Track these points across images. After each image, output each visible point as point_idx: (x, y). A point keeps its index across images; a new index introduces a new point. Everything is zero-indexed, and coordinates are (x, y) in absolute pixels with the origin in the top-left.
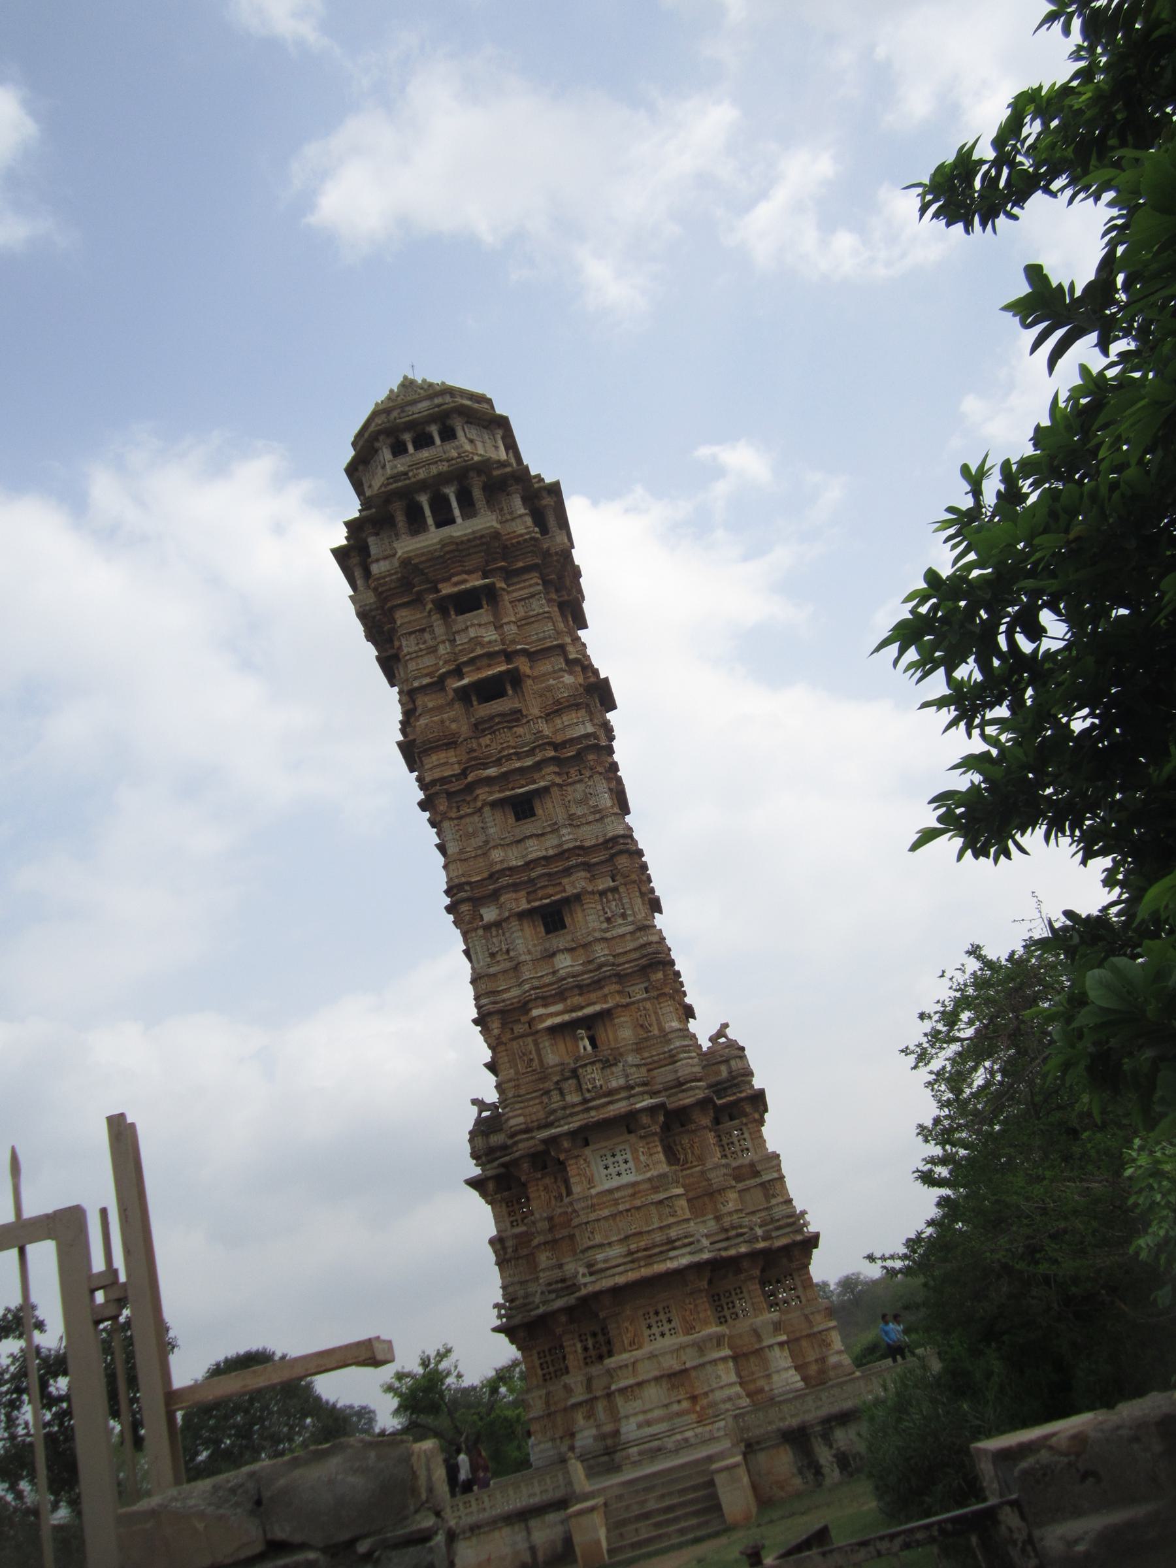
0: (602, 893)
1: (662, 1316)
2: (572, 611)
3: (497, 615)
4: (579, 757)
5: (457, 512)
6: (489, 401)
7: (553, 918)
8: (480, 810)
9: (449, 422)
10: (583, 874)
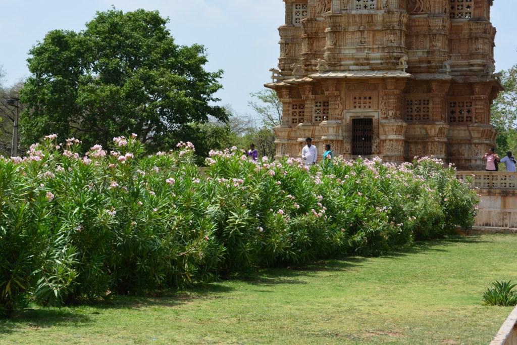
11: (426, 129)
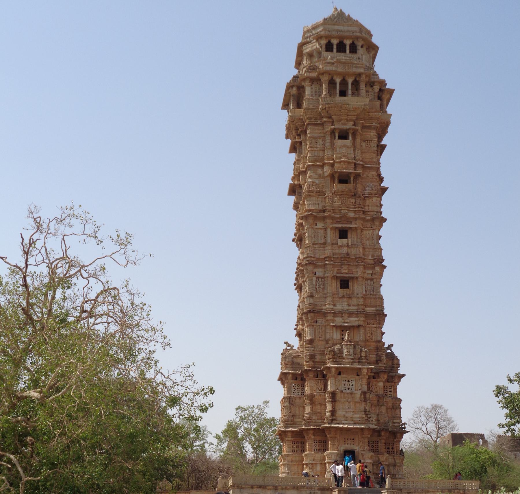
0: (367, 279)
2: (382, 148)
3: (354, 144)
4: (373, 220)
5: (350, 92)
6: (371, 36)
7: (344, 283)
8: (326, 229)
9: (356, 42)
11: (378, 458)
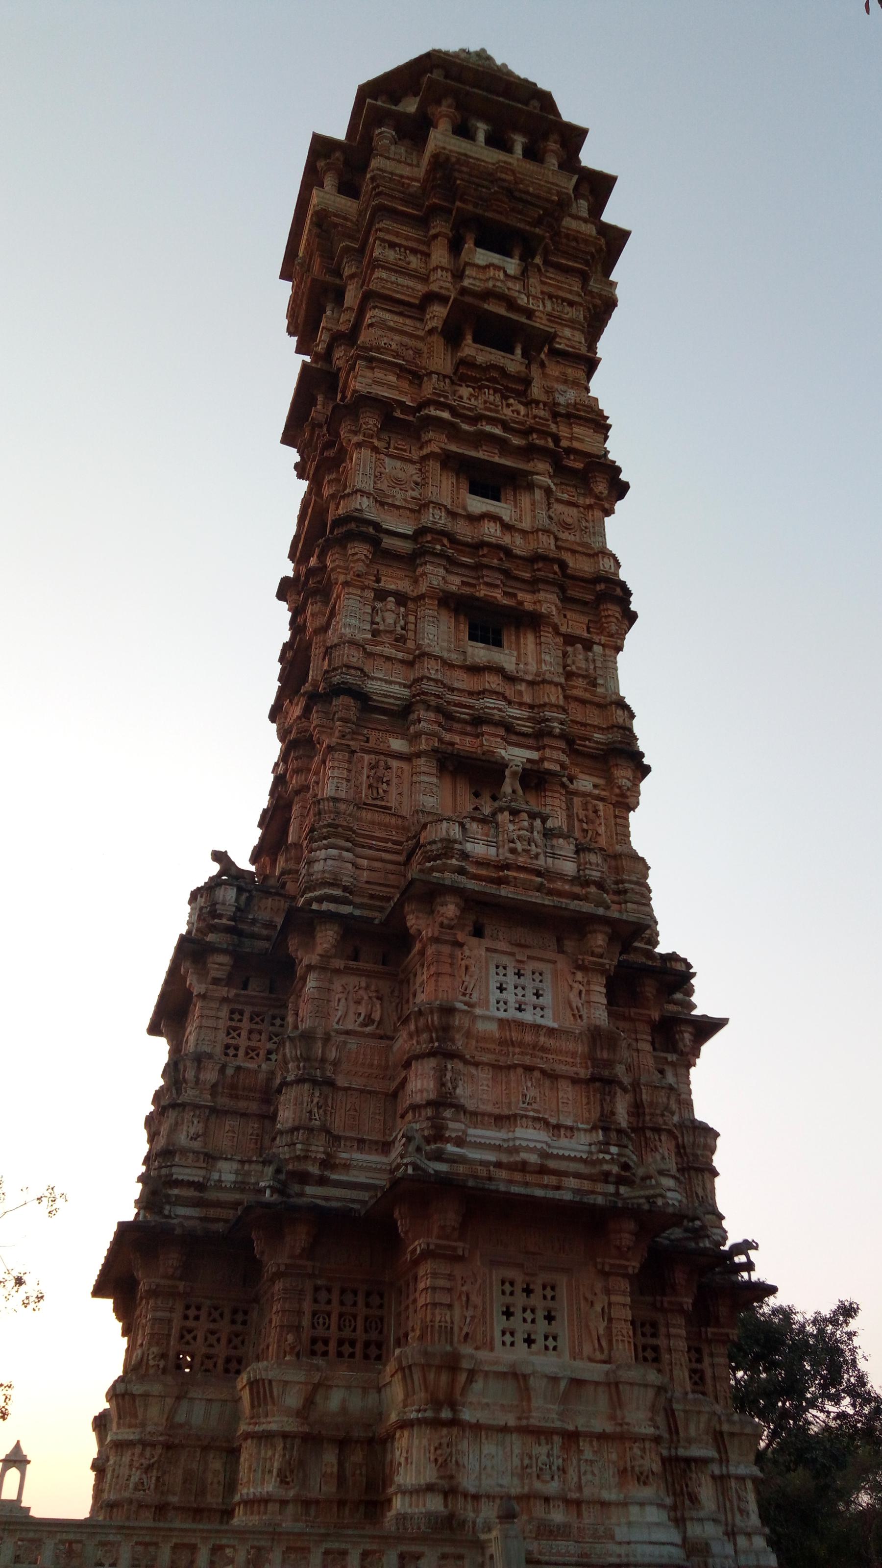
0: (570, 640)
1: (535, 1300)
10: (553, 597)
